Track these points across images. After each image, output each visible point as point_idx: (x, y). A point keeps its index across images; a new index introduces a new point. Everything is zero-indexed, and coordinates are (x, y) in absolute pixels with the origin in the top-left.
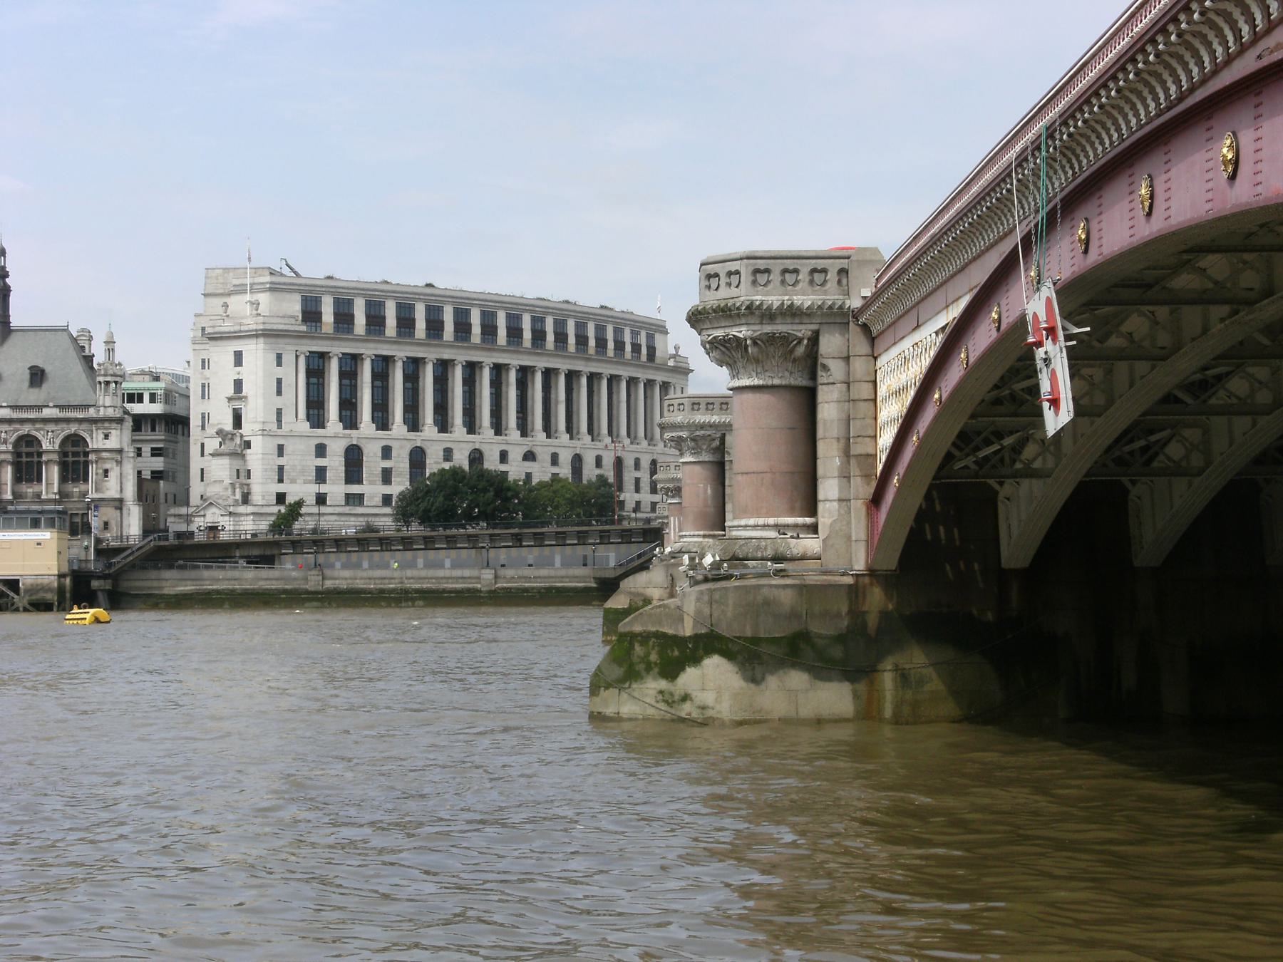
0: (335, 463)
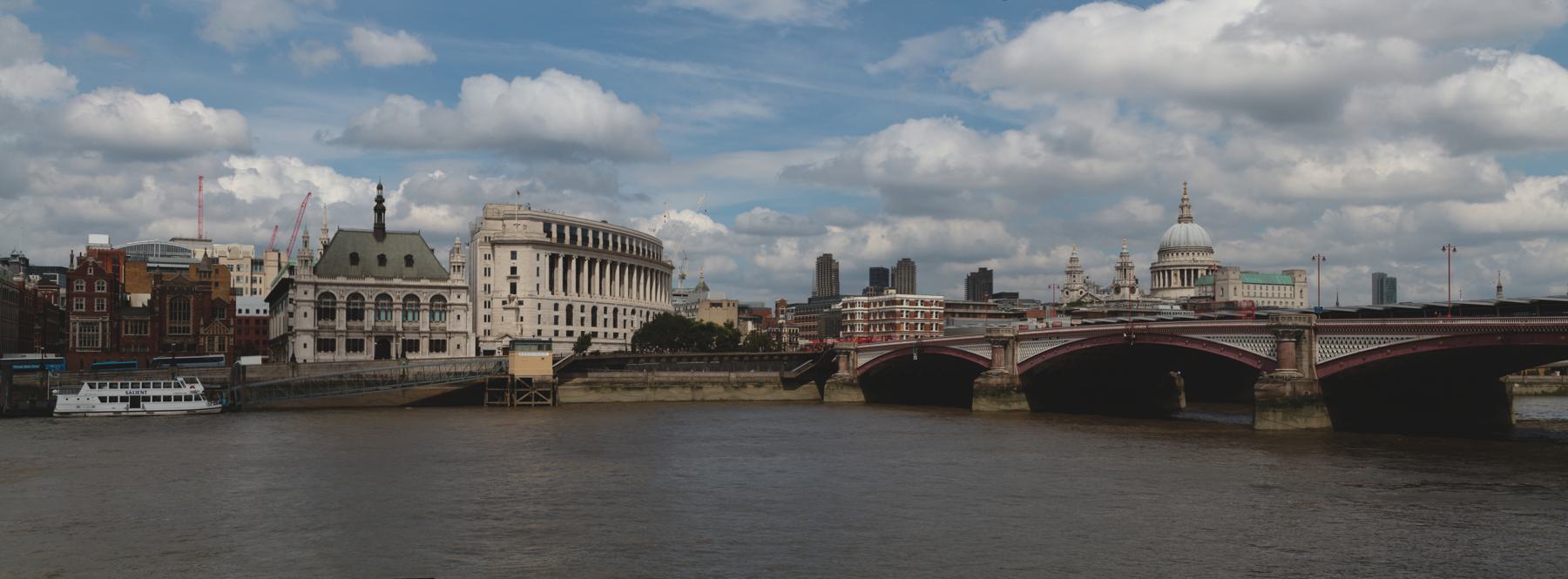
0: (562, 314)
